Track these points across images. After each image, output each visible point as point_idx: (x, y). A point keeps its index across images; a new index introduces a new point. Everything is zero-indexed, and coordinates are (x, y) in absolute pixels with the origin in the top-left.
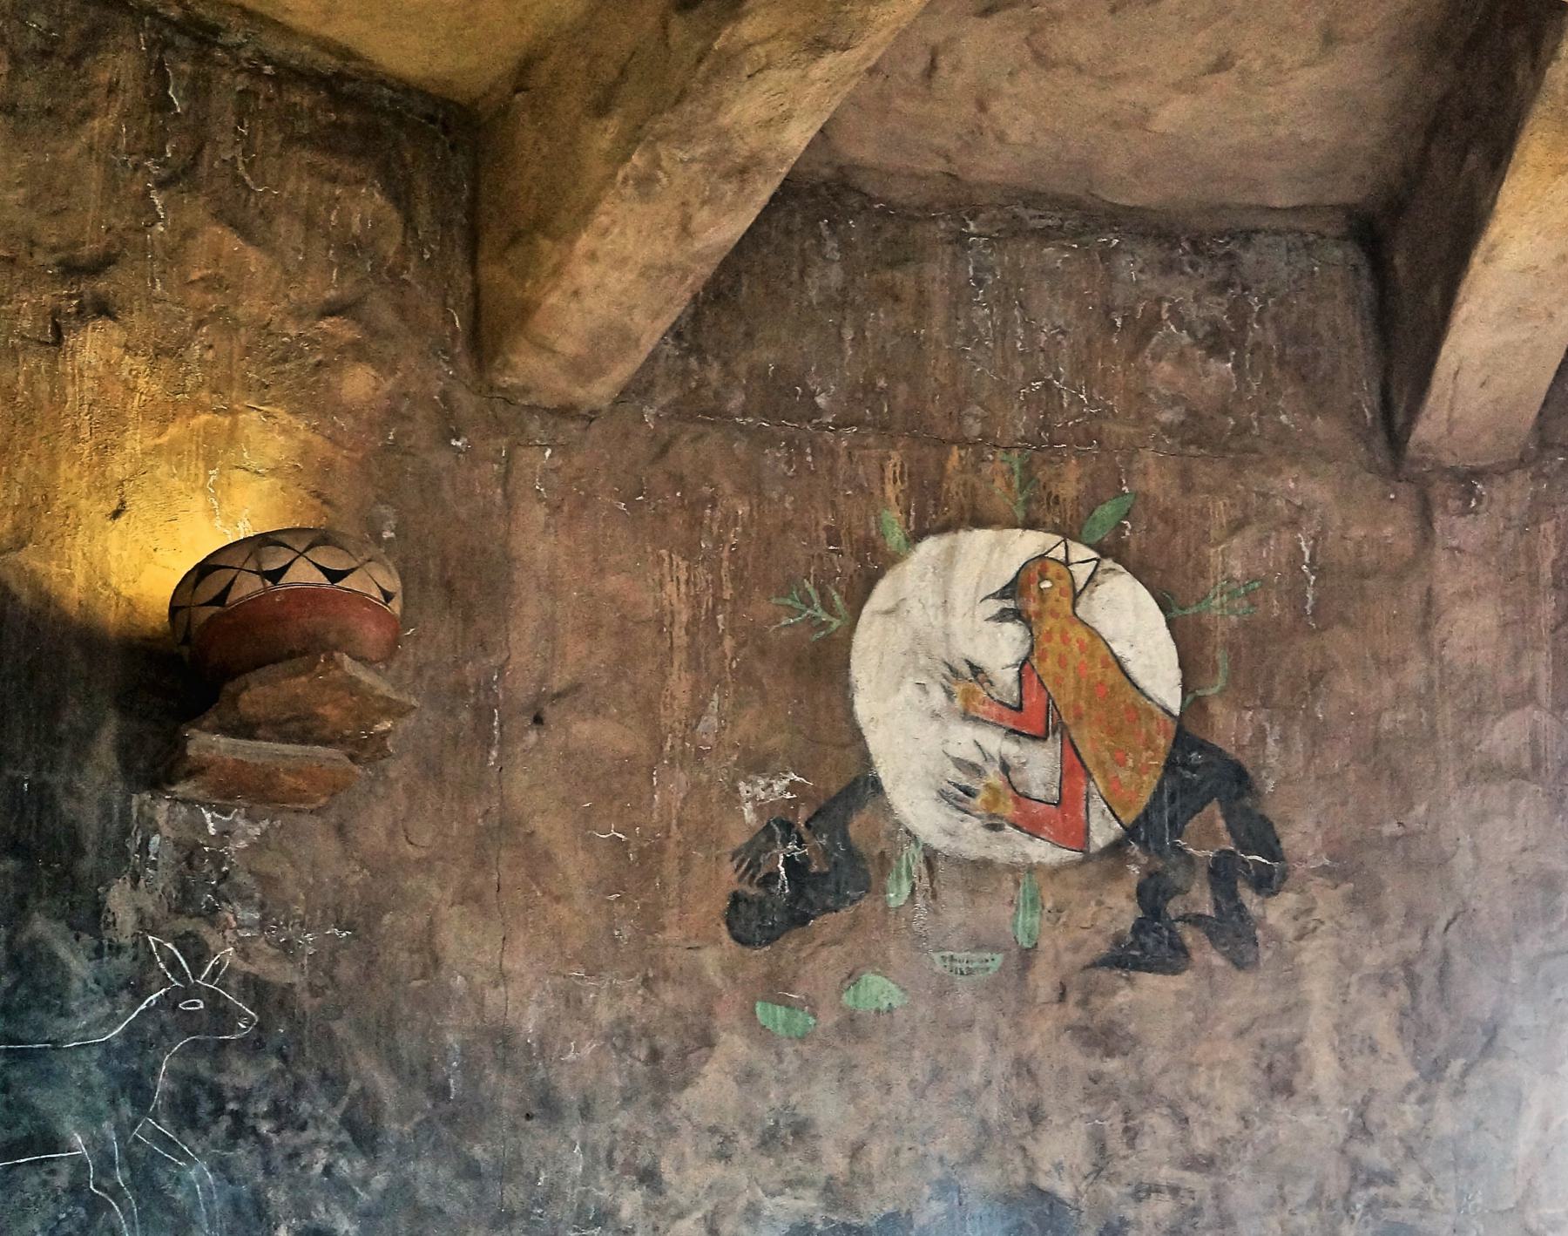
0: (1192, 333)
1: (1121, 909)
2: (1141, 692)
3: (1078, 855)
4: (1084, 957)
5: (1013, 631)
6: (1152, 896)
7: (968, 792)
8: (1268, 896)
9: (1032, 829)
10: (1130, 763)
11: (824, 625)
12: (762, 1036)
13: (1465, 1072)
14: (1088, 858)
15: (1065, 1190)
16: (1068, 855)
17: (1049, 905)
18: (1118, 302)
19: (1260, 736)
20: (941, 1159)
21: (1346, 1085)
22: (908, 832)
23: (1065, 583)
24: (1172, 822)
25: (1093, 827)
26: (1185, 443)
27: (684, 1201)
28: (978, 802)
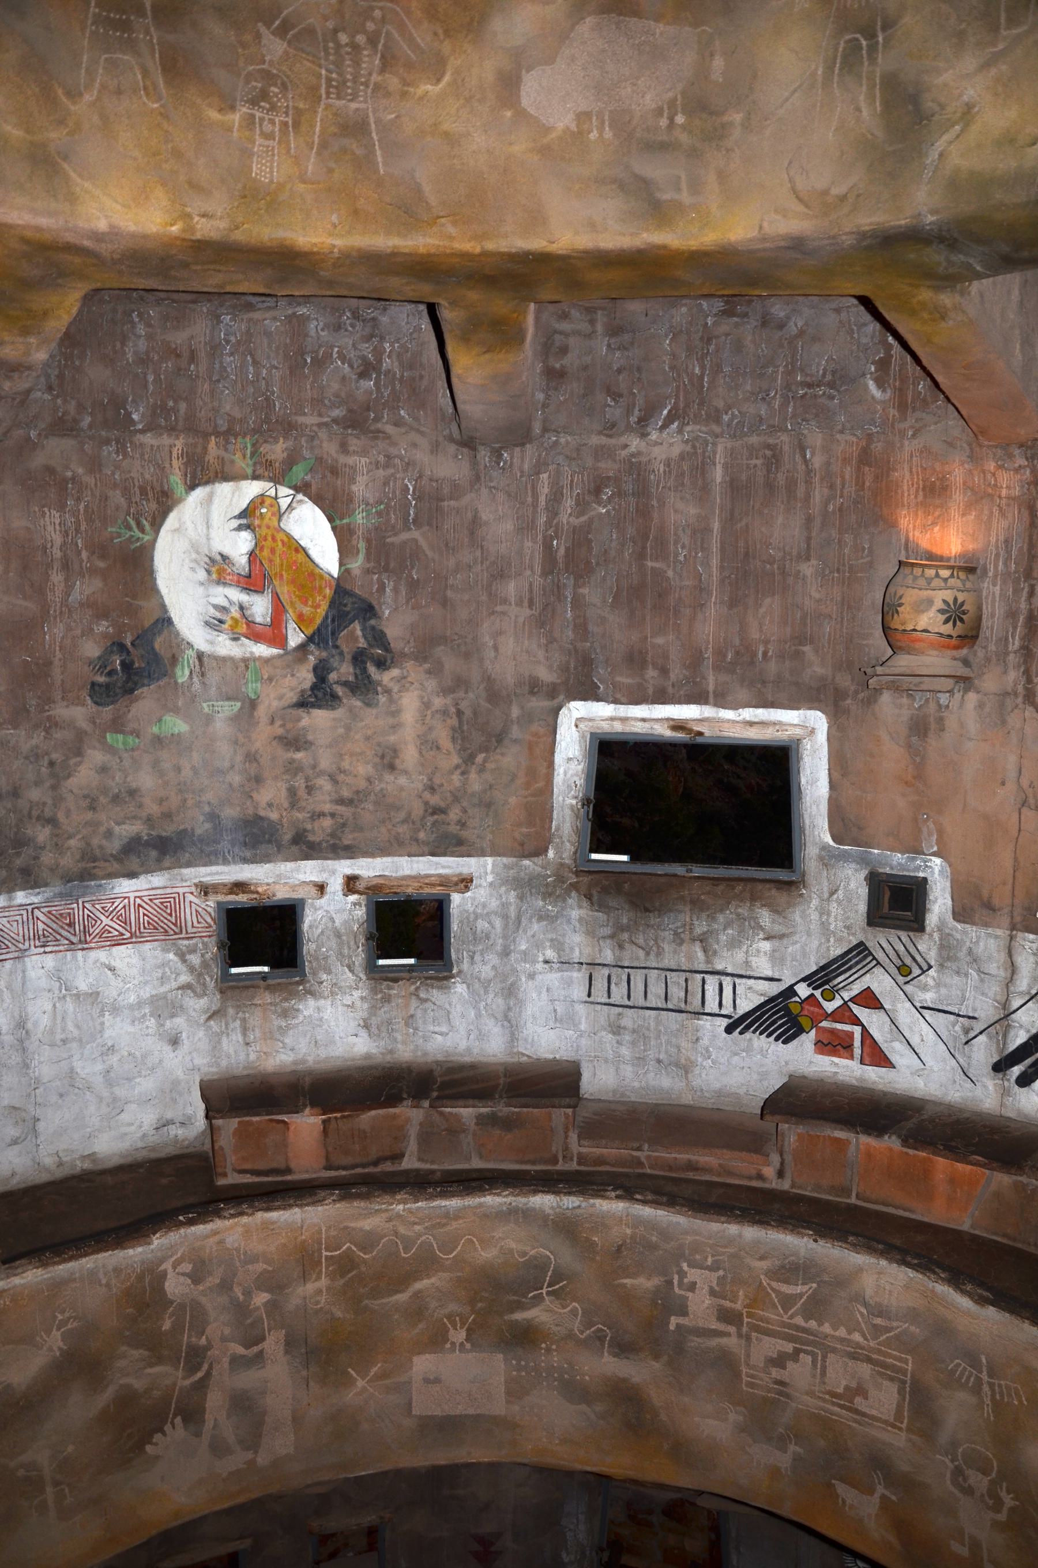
0: (351, 366)
1: (305, 677)
2: (317, 566)
3: (281, 652)
4: (285, 702)
5: (246, 536)
6: (321, 672)
7: (221, 621)
8: (384, 670)
9: (256, 637)
10: (310, 603)
11: (138, 539)
12: (111, 750)
13: (485, 761)
14: (287, 653)
15: (274, 816)
16: (275, 651)
17: (265, 677)
18: (309, 348)
19: (382, 588)
20: (209, 803)
21: (422, 765)
22: (188, 643)
23: (275, 509)
24: (333, 634)
25: (289, 637)
26: (346, 428)
27: (71, 830)
28: (226, 626)
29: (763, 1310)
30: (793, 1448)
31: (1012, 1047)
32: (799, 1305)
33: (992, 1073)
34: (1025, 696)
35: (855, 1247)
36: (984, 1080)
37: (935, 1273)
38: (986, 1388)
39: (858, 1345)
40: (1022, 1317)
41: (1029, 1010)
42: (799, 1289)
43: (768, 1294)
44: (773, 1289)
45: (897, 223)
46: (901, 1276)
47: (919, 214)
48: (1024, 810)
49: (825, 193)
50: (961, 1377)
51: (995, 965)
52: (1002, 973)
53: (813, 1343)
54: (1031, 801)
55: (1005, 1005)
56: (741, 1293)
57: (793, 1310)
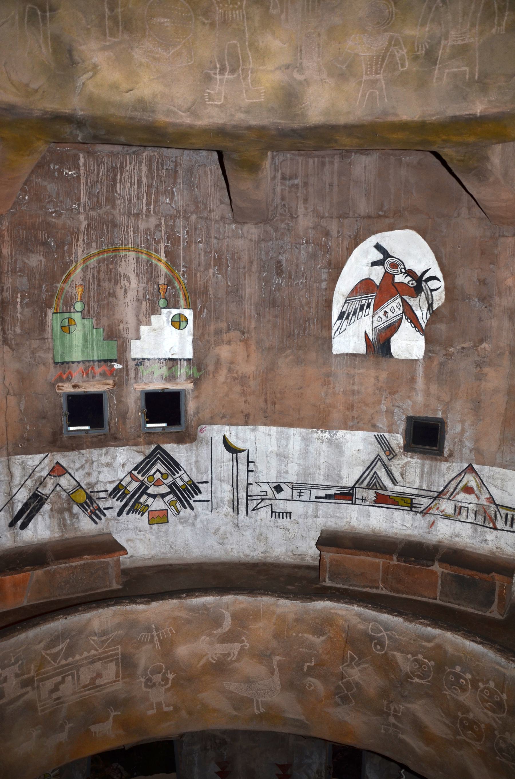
29: (44, 668)
30: (68, 726)
31: (16, 513)
32: (62, 654)
33: (9, 528)
34: (3, 341)
35: (85, 611)
36: (5, 533)
37: (124, 602)
38: (156, 638)
39: (94, 656)
40: (167, 599)
41: (21, 492)
42: (61, 647)
43: (46, 658)
44: (48, 655)
45: (65, 111)
46: (110, 612)
47: (75, 109)
48: (8, 397)
49: (27, 85)
50: (144, 640)
51: (3, 475)
52: (7, 478)
53: (71, 669)
54: (11, 392)
55: (9, 494)
56: (32, 666)
57: (59, 659)
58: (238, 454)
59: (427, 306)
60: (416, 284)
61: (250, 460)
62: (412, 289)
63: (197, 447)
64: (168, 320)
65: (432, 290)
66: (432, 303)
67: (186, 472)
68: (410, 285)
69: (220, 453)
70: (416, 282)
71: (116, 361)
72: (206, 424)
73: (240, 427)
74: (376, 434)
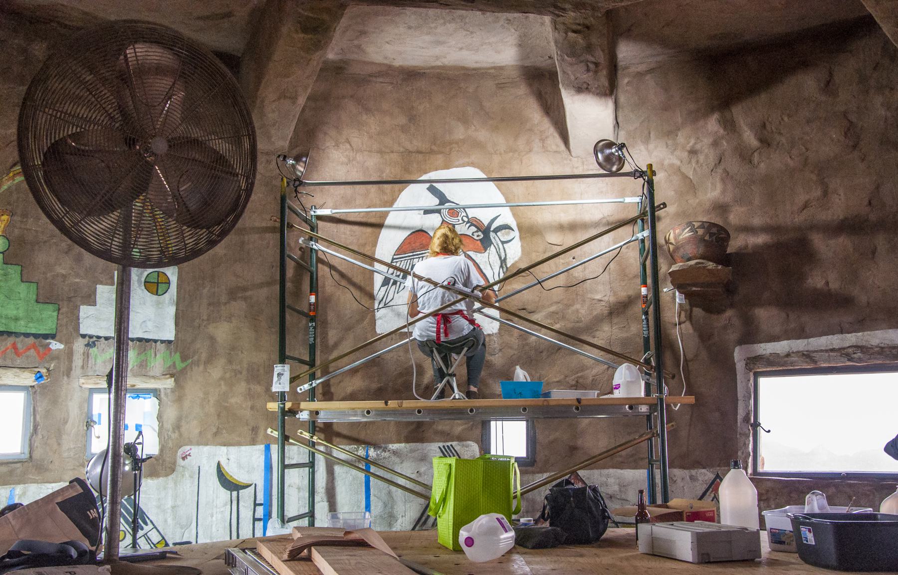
58: (241, 491)
59: (499, 262)
60: (482, 236)
61: (257, 502)
62: (479, 242)
63: (175, 483)
64: (139, 281)
65: (503, 243)
66: (505, 259)
67: (155, 527)
68: (475, 237)
69: (212, 492)
70: (483, 233)
71: (53, 337)
72: (191, 445)
73: (243, 448)
74: (441, 444)
